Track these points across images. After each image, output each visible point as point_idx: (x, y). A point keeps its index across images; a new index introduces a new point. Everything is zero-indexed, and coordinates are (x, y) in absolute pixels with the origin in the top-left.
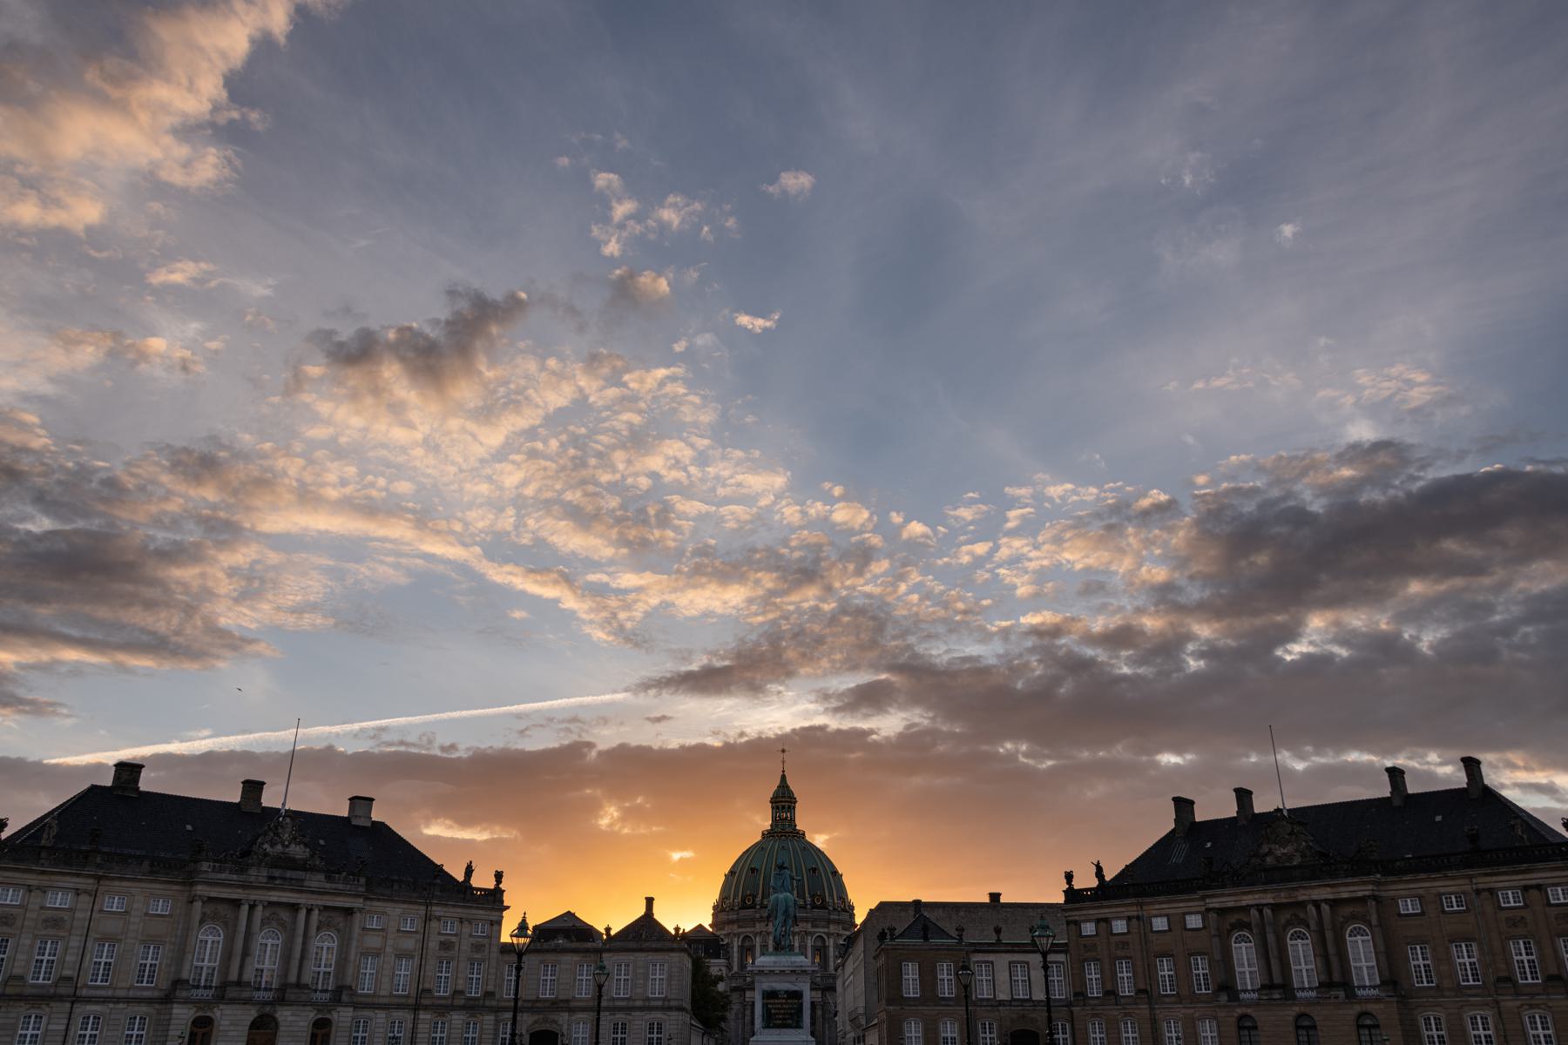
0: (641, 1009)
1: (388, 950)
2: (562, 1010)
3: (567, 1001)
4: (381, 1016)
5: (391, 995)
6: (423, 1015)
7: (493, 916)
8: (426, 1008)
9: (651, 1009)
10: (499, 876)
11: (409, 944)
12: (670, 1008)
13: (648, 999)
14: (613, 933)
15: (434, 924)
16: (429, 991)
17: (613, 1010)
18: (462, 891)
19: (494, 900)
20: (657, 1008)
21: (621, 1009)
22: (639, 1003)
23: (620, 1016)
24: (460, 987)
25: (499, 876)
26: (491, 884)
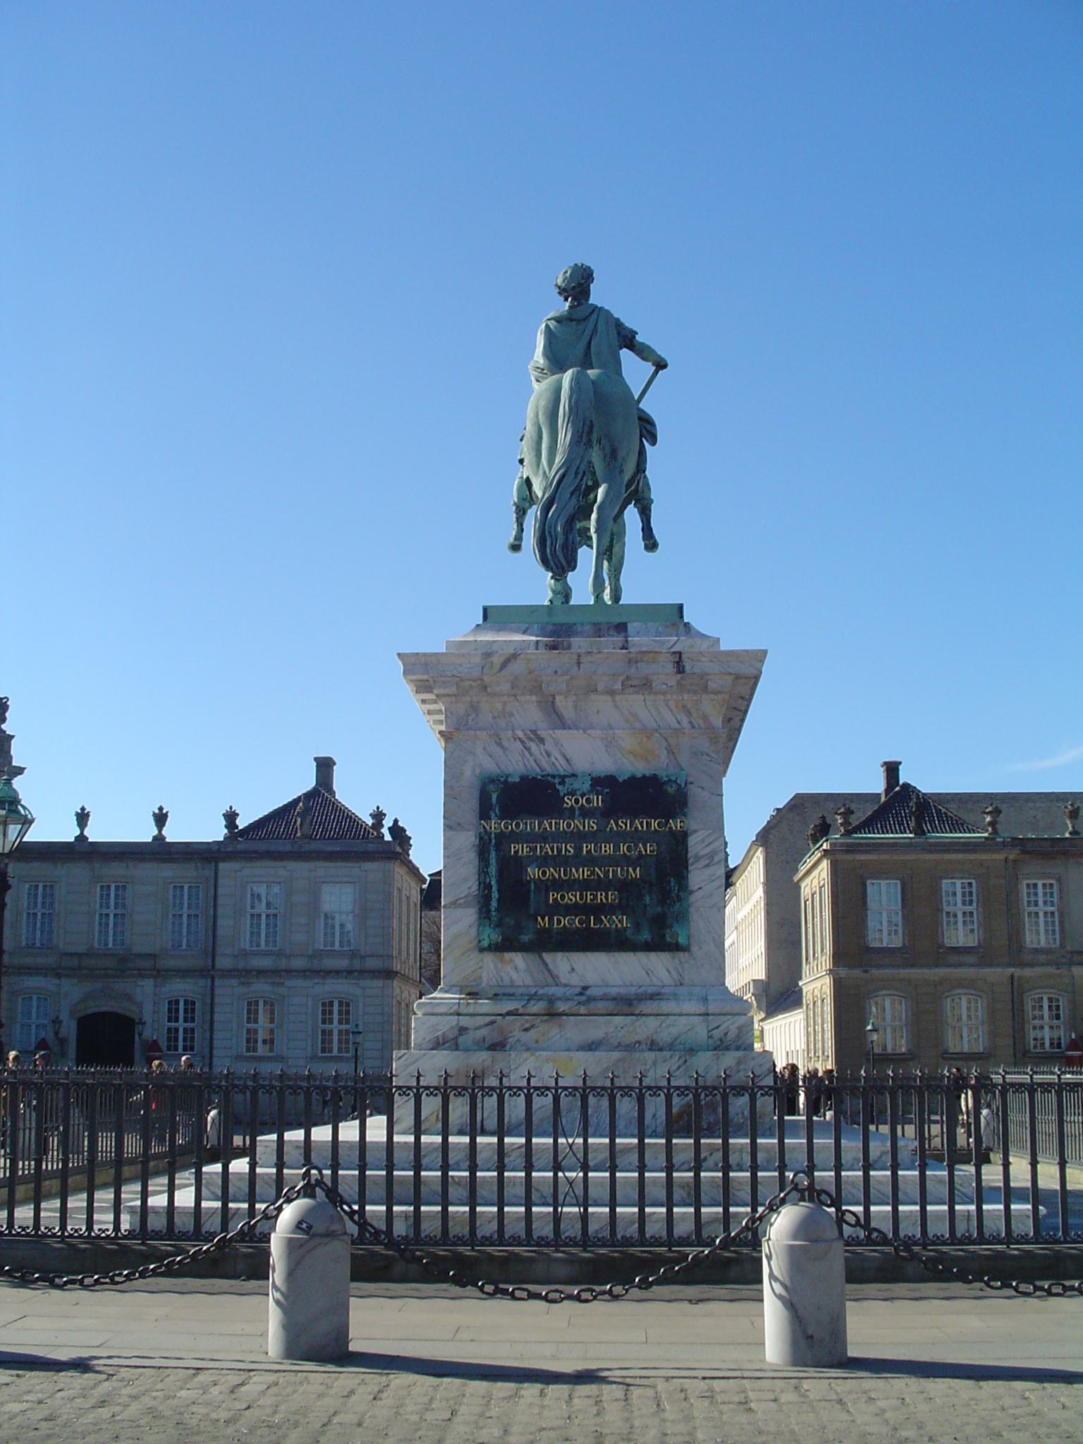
0: (305, 973)
2: (141, 974)
14: (242, 823)
17: (245, 974)
20: (337, 973)
22: (298, 963)
23: (261, 987)
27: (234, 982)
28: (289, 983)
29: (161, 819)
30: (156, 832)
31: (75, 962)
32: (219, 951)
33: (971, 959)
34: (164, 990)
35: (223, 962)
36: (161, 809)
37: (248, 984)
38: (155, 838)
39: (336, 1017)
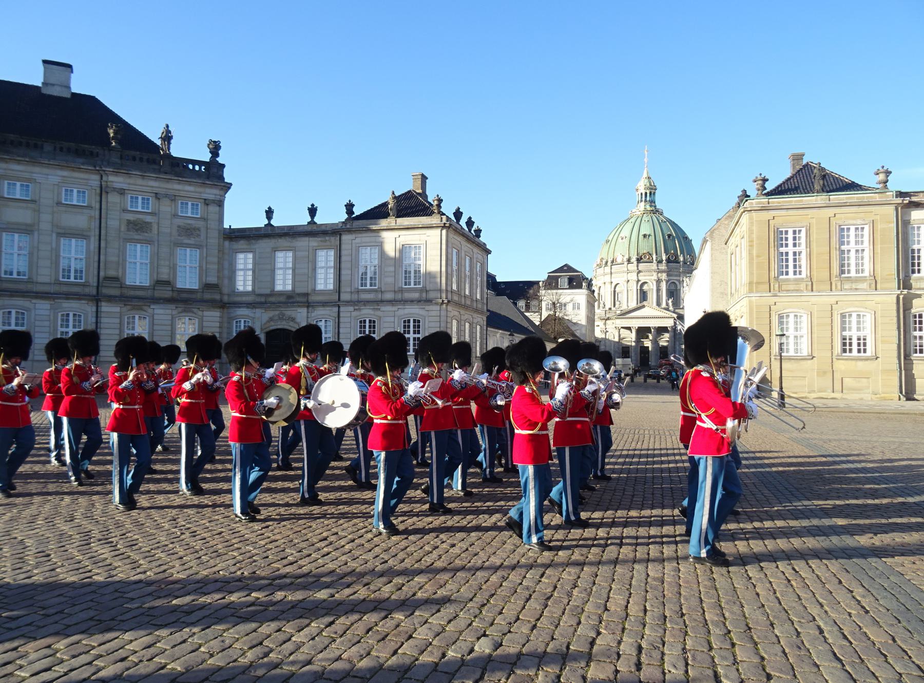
0: (392, 302)
1: (45, 226)
2: (300, 304)
3: (307, 295)
4: (43, 307)
5: (61, 283)
6: (105, 307)
7: (211, 193)
8: (111, 299)
9: (405, 302)
10: (215, 148)
11: (80, 221)
12: (429, 301)
13: (401, 290)
14: (357, 211)
15: (113, 198)
16: (116, 279)
17: (357, 303)
18: (143, 154)
19: (212, 173)
21: (367, 302)
22: (389, 296)
24: (164, 277)
25: (215, 148)
26: (206, 157)
27: (351, 309)
28: (383, 308)
29: (313, 211)
30: (310, 220)
31: (263, 300)
32: (342, 290)
33: (860, 286)
34: (313, 315)
35: (345, 297)
36: (313, 205)
37: (359, 310)
38: (309, 223)
39: (412, 329)
